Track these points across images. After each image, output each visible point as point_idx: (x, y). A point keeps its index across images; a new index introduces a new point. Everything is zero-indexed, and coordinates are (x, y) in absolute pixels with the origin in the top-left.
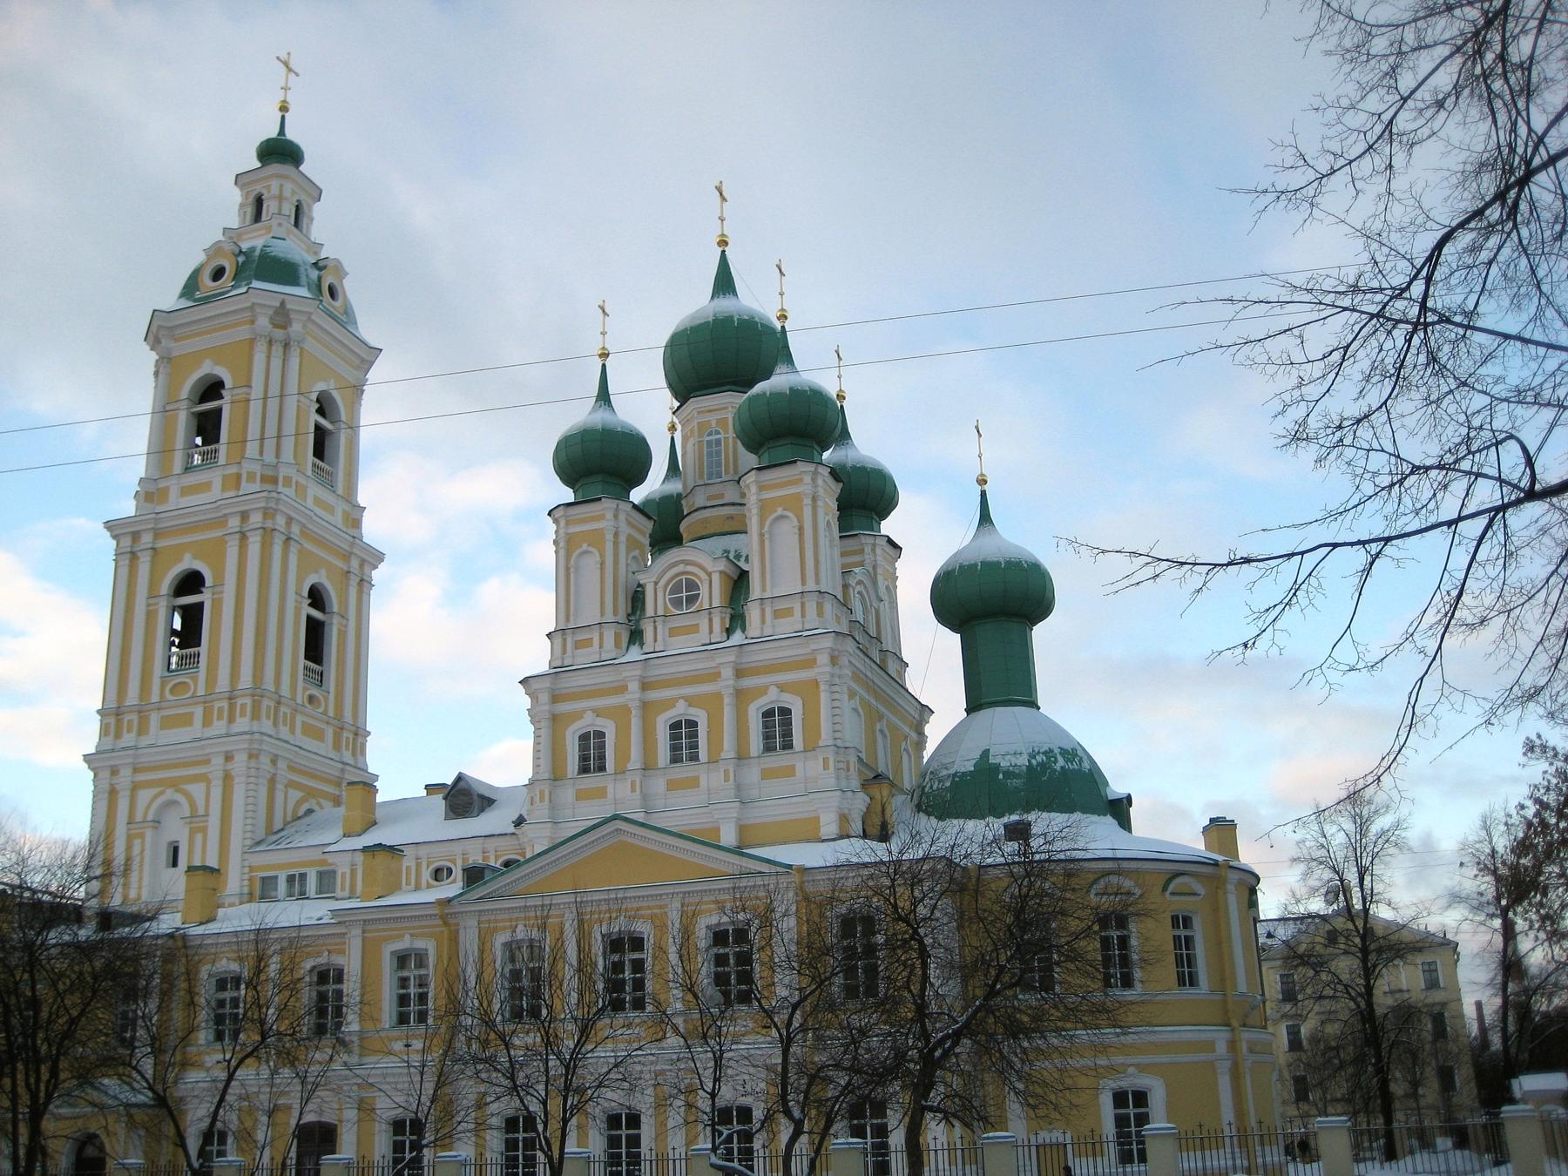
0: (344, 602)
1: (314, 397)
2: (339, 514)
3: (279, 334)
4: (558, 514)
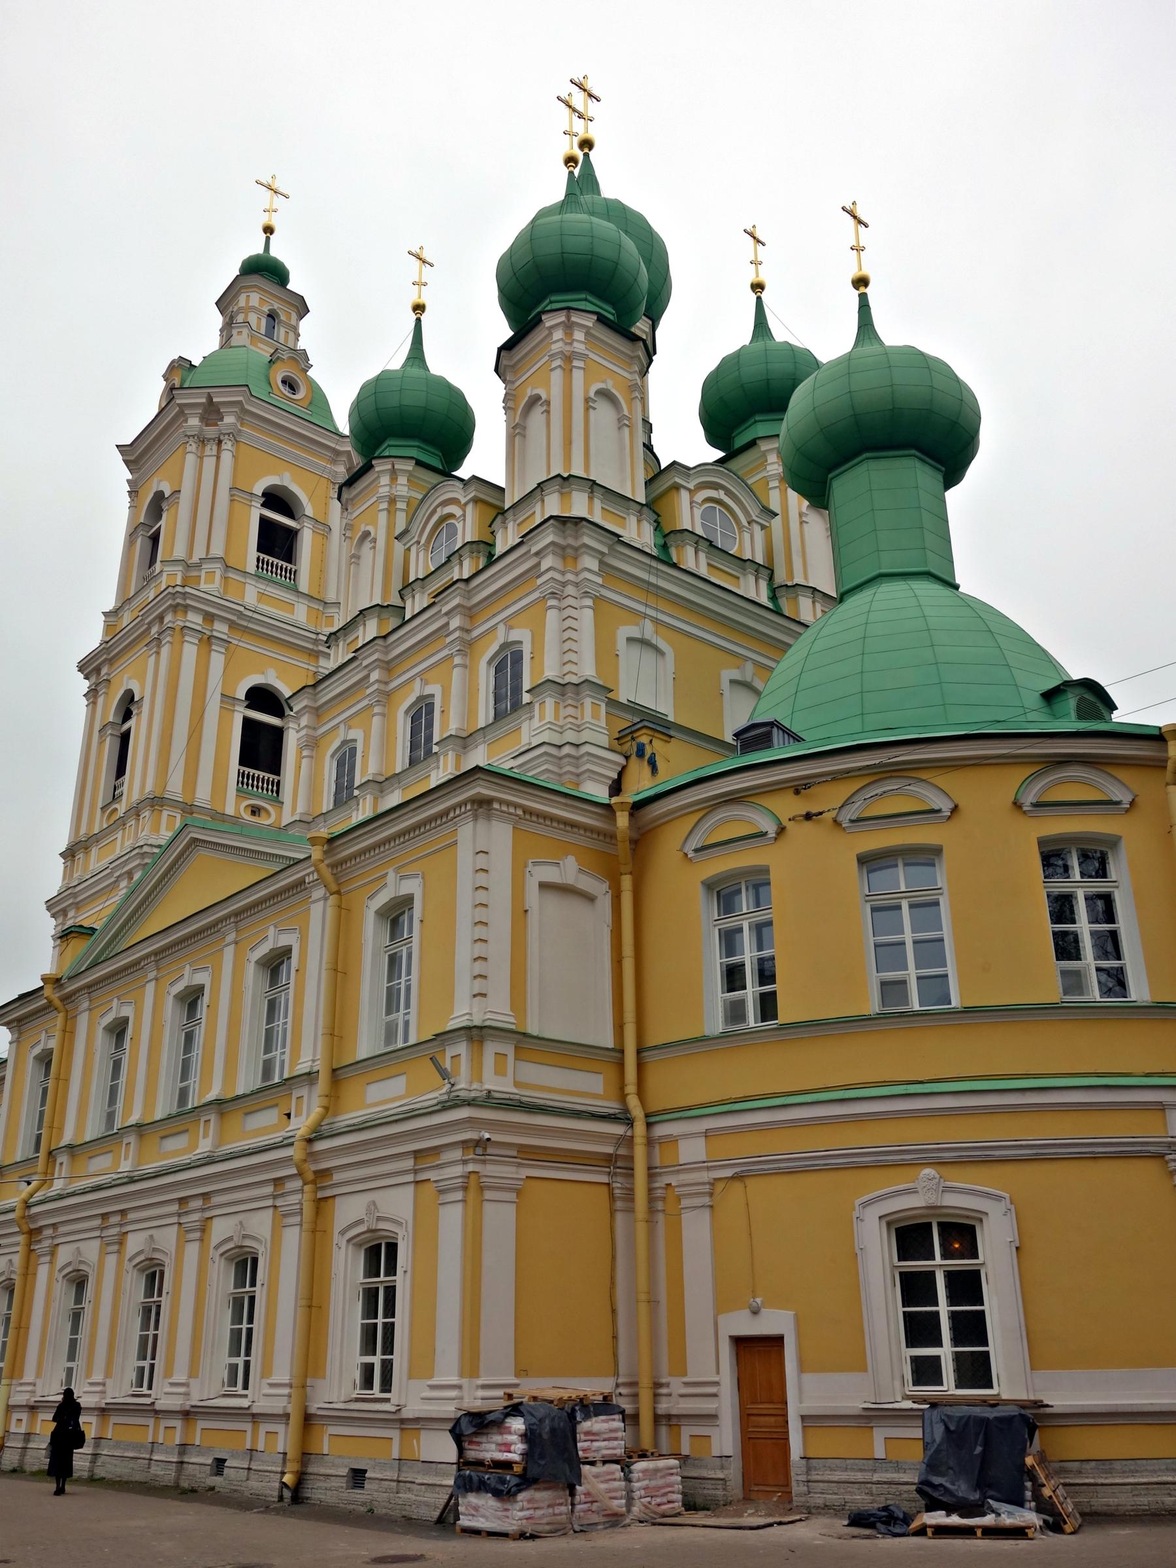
3: (211, 432)
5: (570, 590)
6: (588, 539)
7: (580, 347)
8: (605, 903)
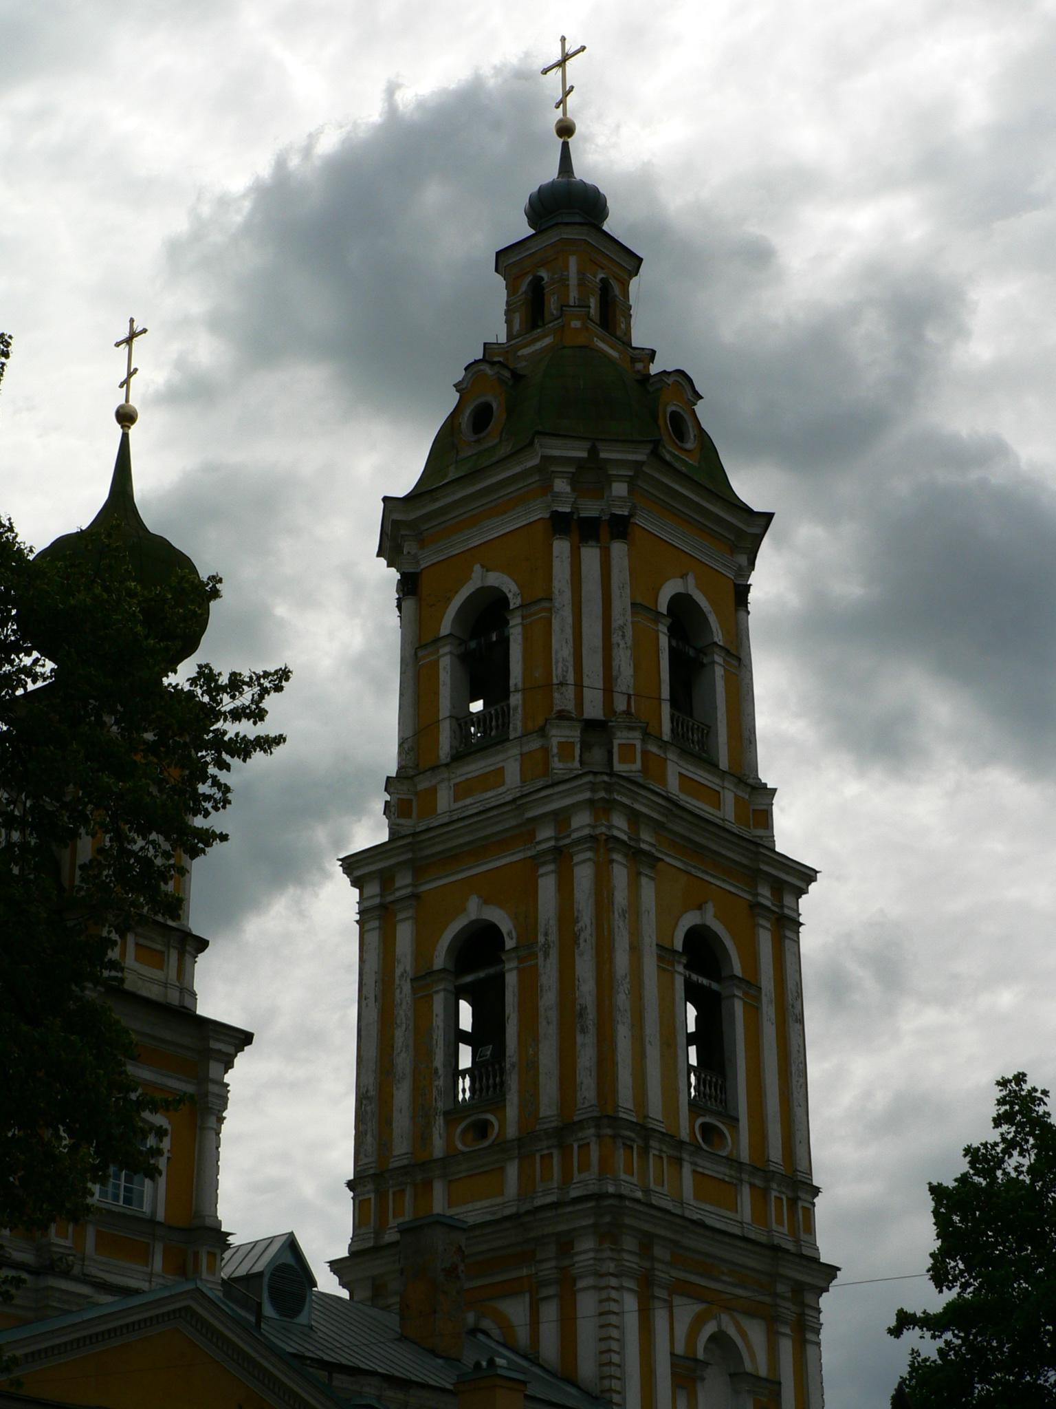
0: (752, 959)
1: (663, 608)
2: (728, 798)
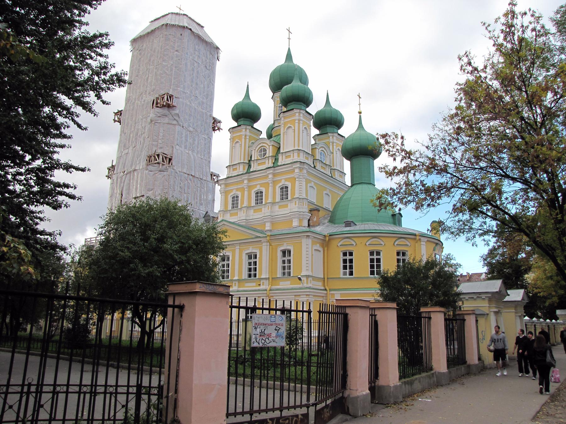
4: (231, 130)
5: (301, 177)
6: (306, 166)
7: (302, 118)
8: (322, 252)
